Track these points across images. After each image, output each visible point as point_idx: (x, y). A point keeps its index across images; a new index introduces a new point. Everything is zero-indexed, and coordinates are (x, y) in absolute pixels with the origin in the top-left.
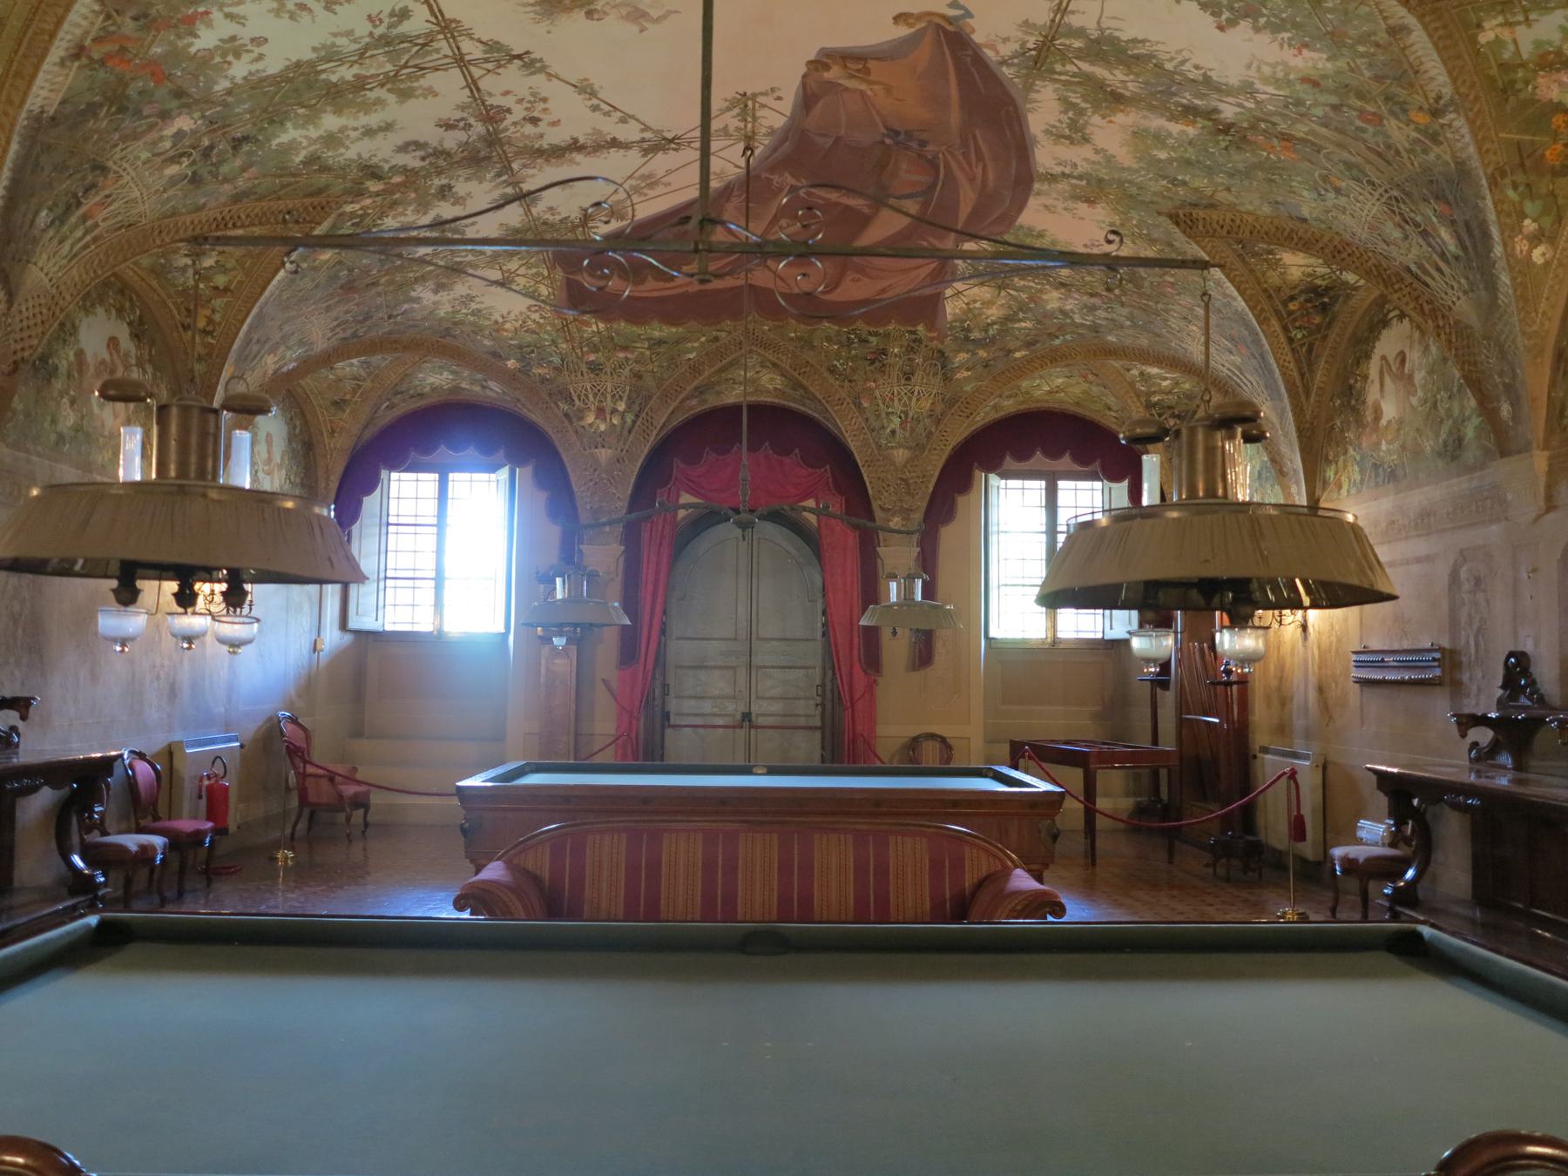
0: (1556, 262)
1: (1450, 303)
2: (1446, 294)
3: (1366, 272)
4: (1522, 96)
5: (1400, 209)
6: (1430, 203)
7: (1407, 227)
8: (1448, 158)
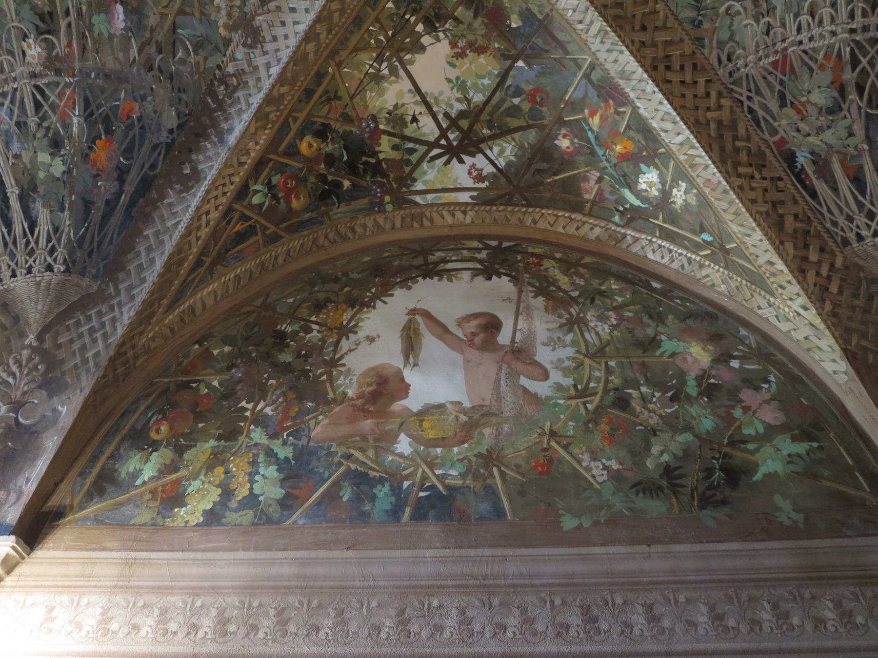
1: (851, 236)
2: (850, 219)
3: (697, 121)
7: (853, 96)
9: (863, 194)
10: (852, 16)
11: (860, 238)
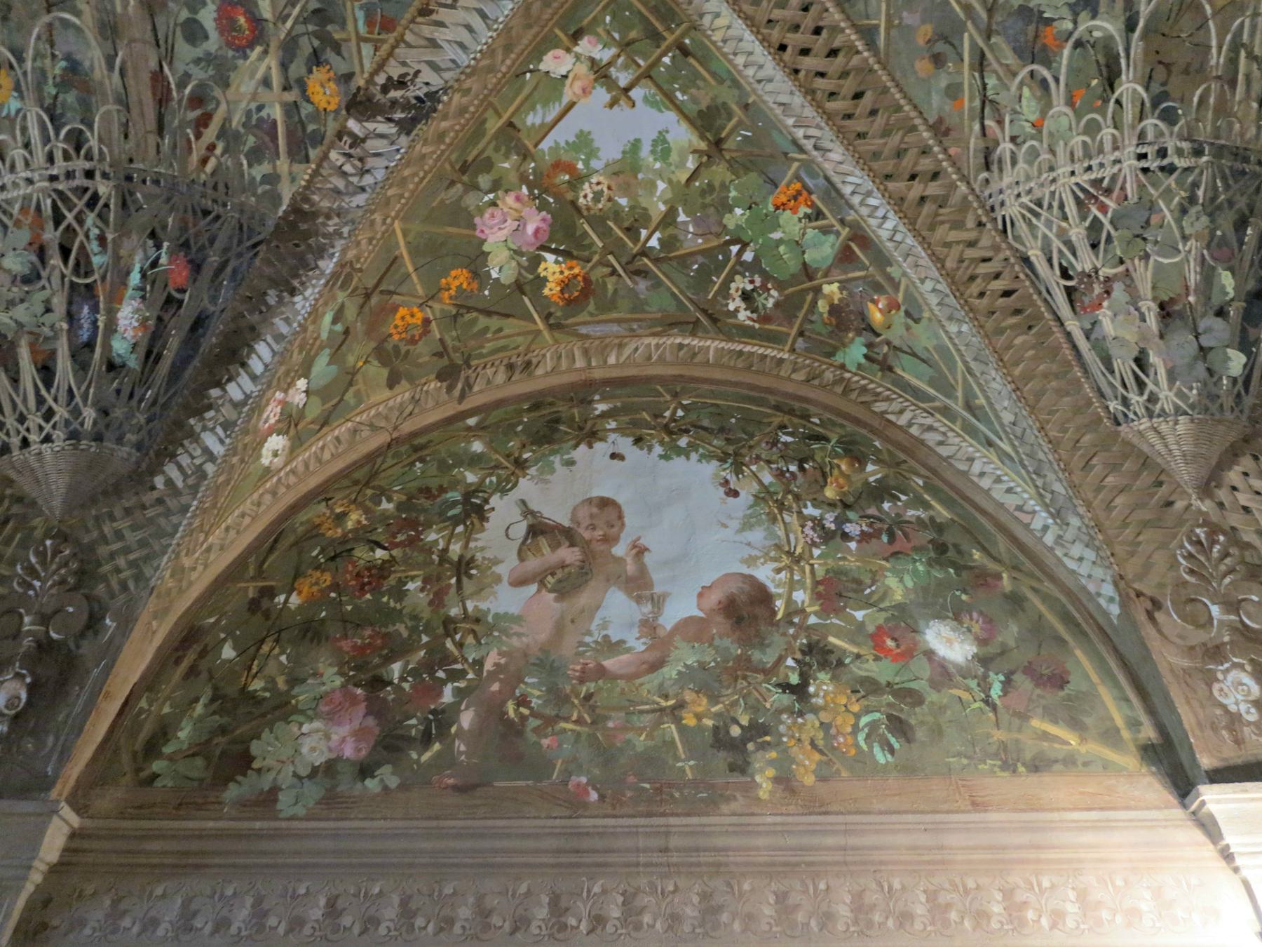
0: (275, 479)
1: (15, 441)
2: (22, 419)
4: (471, 200)
5: (80, 219)
6: (158, 247)
7: (55, 261)
8: (287, 192)
9: (48, 385)
10: (51, 159)
11: (25, 443)
